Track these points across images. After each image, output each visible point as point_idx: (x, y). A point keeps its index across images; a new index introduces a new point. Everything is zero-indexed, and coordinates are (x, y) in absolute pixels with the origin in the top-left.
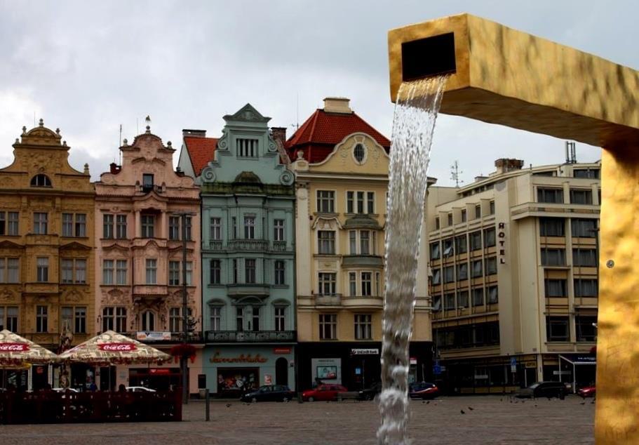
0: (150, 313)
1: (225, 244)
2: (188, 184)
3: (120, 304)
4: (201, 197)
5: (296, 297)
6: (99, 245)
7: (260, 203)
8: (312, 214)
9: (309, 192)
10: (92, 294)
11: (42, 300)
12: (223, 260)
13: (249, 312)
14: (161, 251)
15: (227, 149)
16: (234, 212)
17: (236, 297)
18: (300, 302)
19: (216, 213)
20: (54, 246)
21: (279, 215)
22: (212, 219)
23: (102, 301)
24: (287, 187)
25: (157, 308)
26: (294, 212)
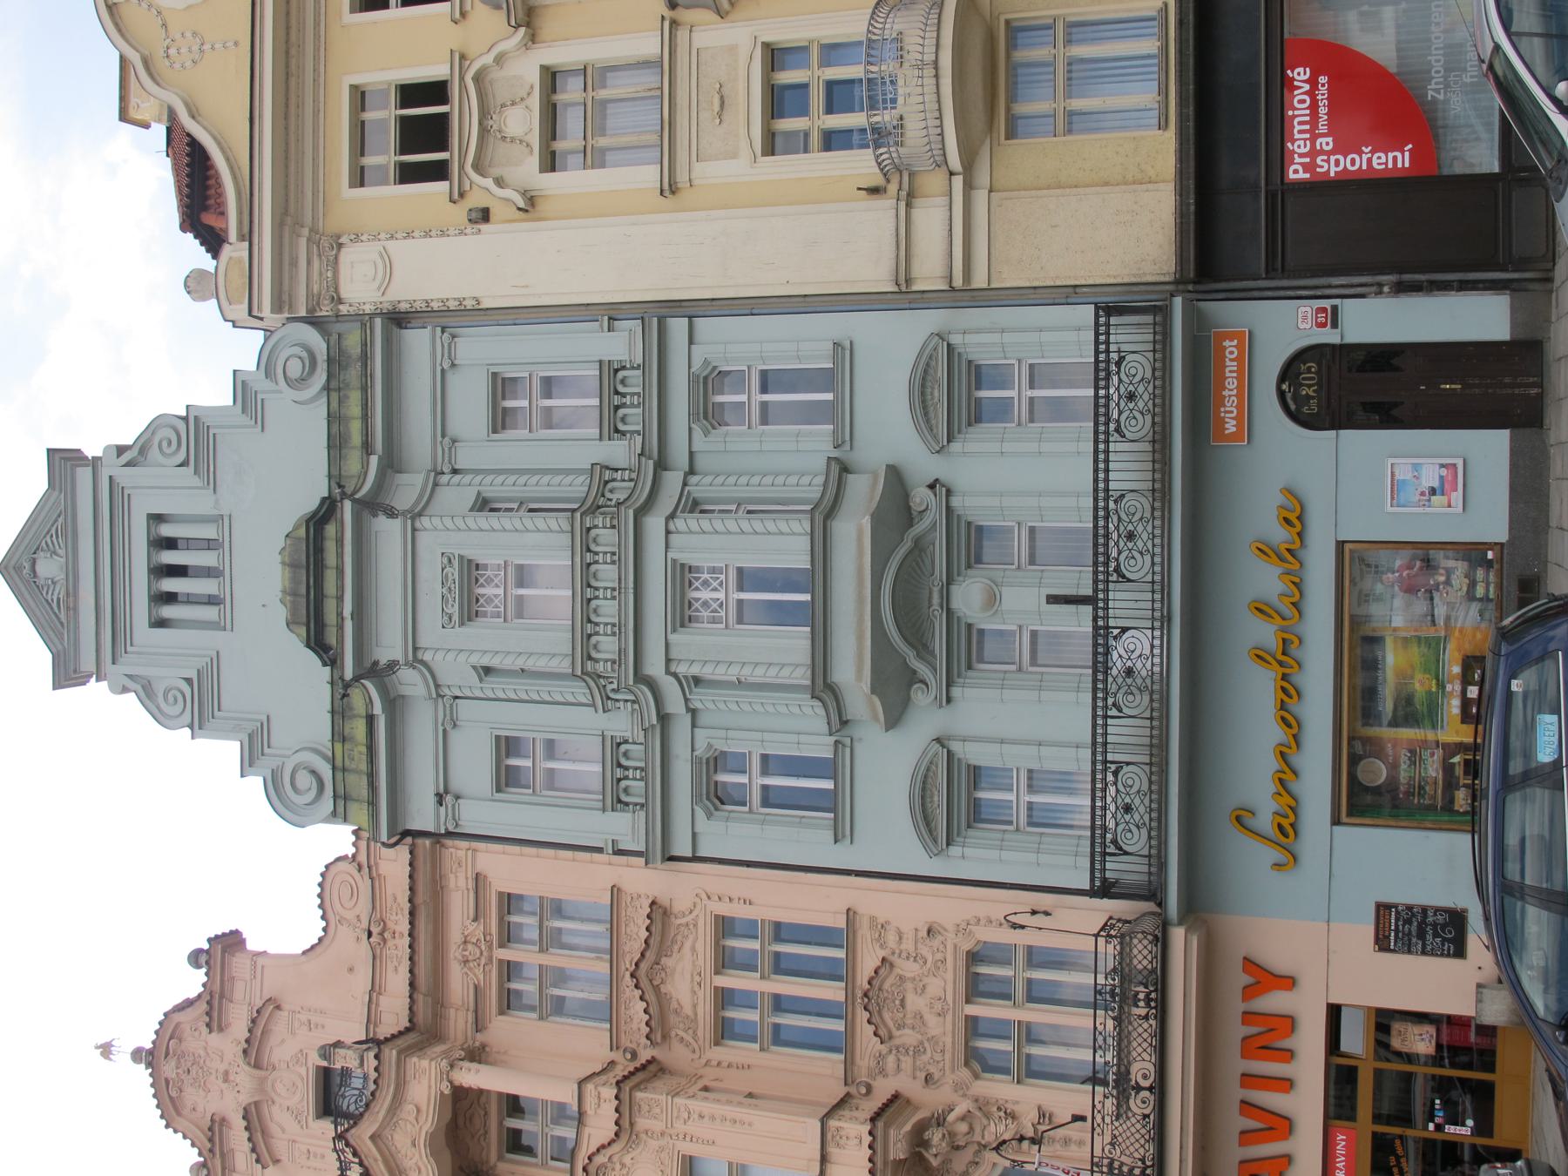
2: (354, 892)
5: (904, 295)
7: (389, 532)
8: (459, 213)
9: (357, 238)
14: (642, 1123)
15: (189, 681)
19: (473, 766)
21: (470, 405)
24: (336, 362)
26: (449, 319)
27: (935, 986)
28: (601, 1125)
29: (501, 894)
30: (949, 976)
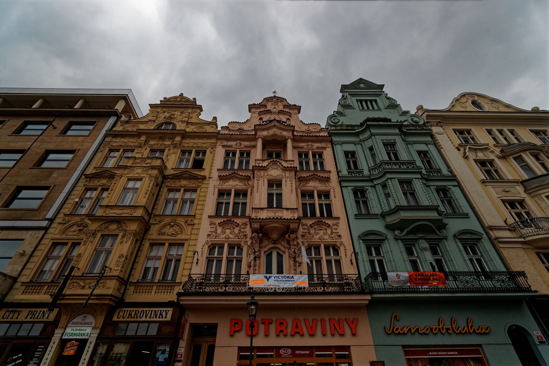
0: (278, 253)
1: (366, 172)
3: (233, 239)
4: (330, 135)
6: (215, 175)
10: (195, 227)
11: (114, 227)
12: (369, 188)
13: (425, 249)
16: (368, 144)
17: (401, 225)
18: (495, 234)
19: (350, 148)
20: (153, 168)
22: (346, 154)
23: (209, 235)
25: (286, 245)
27: (326, 237)
28: (285, 164)
29: (323, 152)
30: (329, 240)
